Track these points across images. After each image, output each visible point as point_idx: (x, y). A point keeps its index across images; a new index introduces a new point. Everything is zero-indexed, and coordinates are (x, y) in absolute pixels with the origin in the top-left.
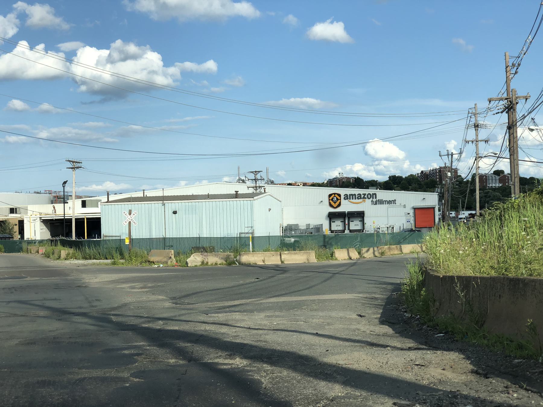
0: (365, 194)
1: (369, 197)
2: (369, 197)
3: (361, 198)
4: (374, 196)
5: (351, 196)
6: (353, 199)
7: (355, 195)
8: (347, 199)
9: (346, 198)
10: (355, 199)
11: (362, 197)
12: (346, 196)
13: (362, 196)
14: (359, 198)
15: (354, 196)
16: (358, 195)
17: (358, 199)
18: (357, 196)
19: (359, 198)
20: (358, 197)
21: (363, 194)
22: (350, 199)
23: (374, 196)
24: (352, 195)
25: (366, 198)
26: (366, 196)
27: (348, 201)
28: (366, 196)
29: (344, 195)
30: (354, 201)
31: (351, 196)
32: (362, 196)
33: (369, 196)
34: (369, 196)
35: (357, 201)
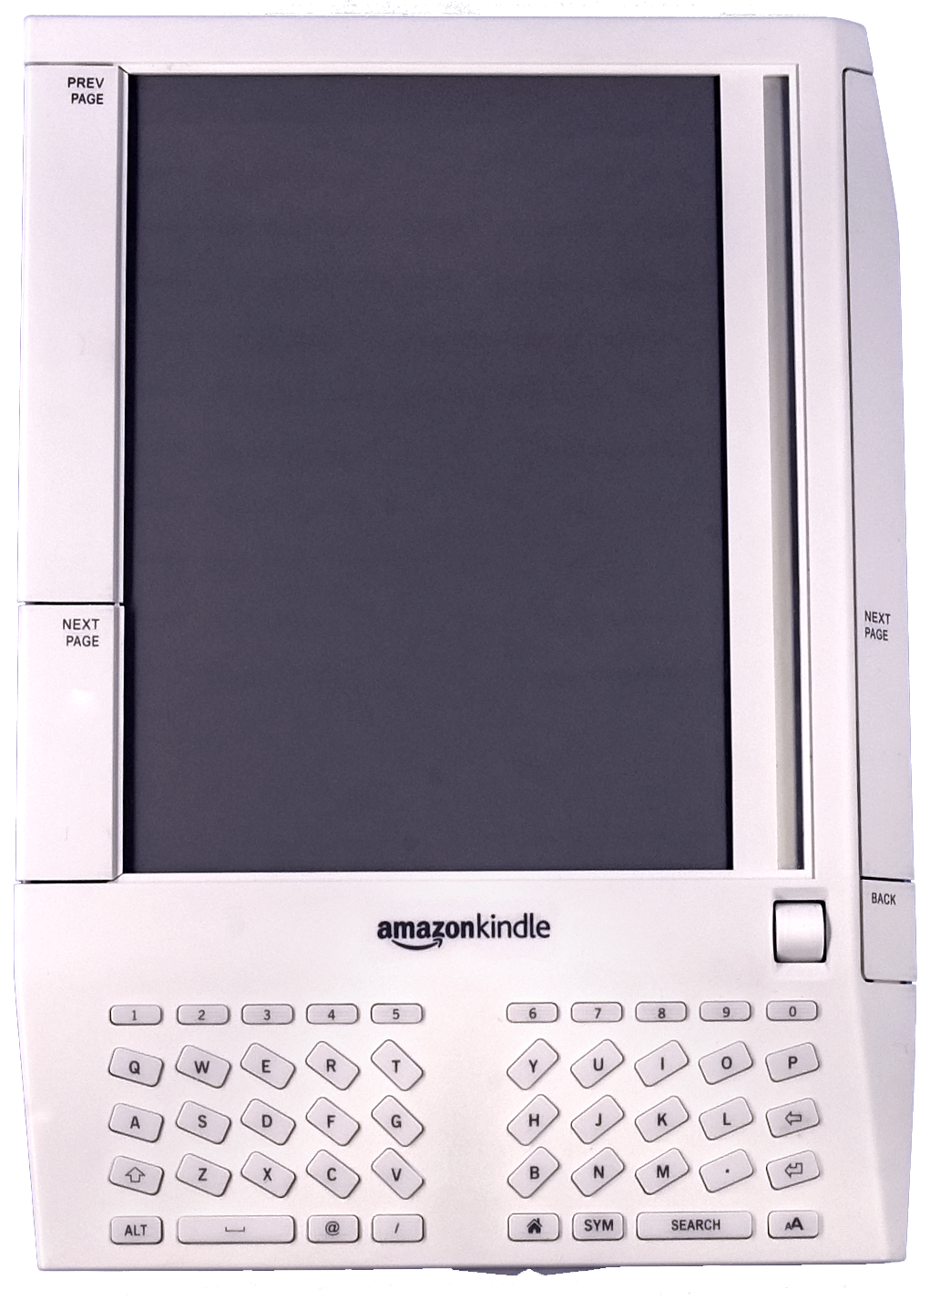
0: (440, 924)
3: (428, 935)
4: (467, 928)
6: (404, 936)
7: (411, 924)
8: (390, 936)
9: (384, 933)
10: (412, 936)
11: (431, 933)
13: (433, 928)
14: (423, 933)
15: (408, 928)
16: (420, 925)
17: (420, 936)
18: (416, 929)
19: (423, 933)
20: (419, 932)
21: (435, 923)
22: (397, 936)
23: (467, 928)
24: (404, 925)
25: (443, 935)
26: (443, 930)
27: (393, 941)
28: (443, 930)
29: (381, 925)
30: (408, 941)
32: (433, 928)
35: (417, 941)
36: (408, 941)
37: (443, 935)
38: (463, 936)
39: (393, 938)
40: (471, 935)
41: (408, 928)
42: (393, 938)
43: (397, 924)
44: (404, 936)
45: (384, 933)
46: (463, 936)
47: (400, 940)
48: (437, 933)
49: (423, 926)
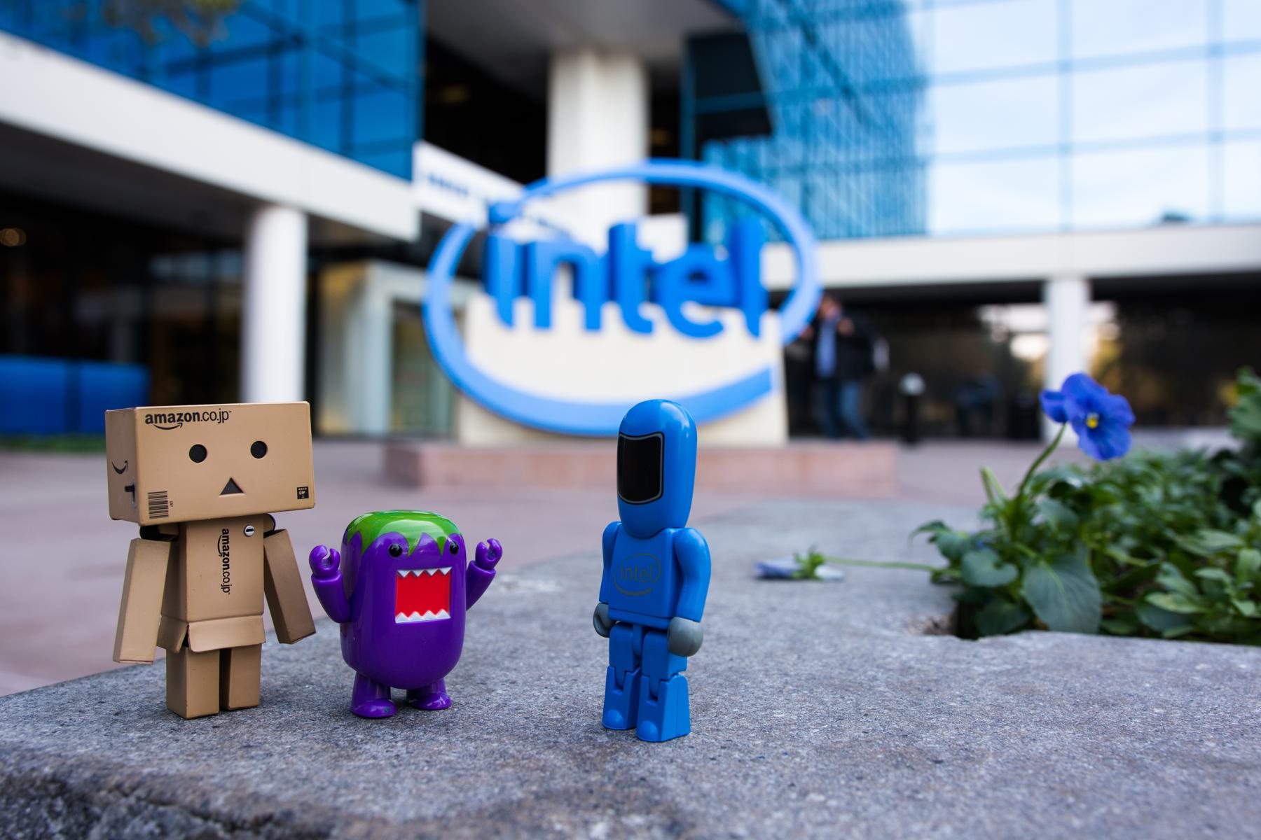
0: (181, 415)
1: (188, 418)
2: (188, 418)
3: (174, 421)
4: (196, 416)
5: (158, 418)
6: (161, 422)
7: (164, 415)
8: (152, 422)
9: (149, 421)
10: (165, 422)
12: (149, 417)
13: (177, 417)
14: (171, 420)
15: (163, 418)
16: (169, 415)
17: (170, 422)
18: (167, 418)
19: (171, 420)
20: (169, 419)
21: (178, 414)
22: (156, 422)
23: (196, 416)
24: (160, 416)
25: (182, 421)
26: (183, 418)
28: (183, 418)
29: (147, 416)
30: (163, 425)
31: (158, 418)
32: (177, 417)
33: (188, 416)
34: (188, 416)
35: (168, 425)
36: (163, 425)
37: (182, 421)
38: (194, 420)
39: (154, 423)
40: (199, 420)
41: (163, 418)
42: (154, 423)
43: (156, 416)
44: (161, 422)
45: (149, 421)
46: (194, 420)
47: (158, 424)
48: (179, 420)
49: (171, 416)
